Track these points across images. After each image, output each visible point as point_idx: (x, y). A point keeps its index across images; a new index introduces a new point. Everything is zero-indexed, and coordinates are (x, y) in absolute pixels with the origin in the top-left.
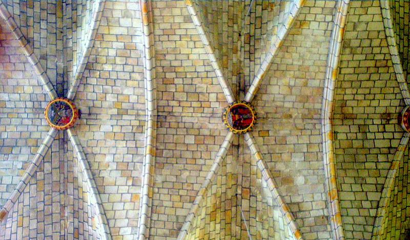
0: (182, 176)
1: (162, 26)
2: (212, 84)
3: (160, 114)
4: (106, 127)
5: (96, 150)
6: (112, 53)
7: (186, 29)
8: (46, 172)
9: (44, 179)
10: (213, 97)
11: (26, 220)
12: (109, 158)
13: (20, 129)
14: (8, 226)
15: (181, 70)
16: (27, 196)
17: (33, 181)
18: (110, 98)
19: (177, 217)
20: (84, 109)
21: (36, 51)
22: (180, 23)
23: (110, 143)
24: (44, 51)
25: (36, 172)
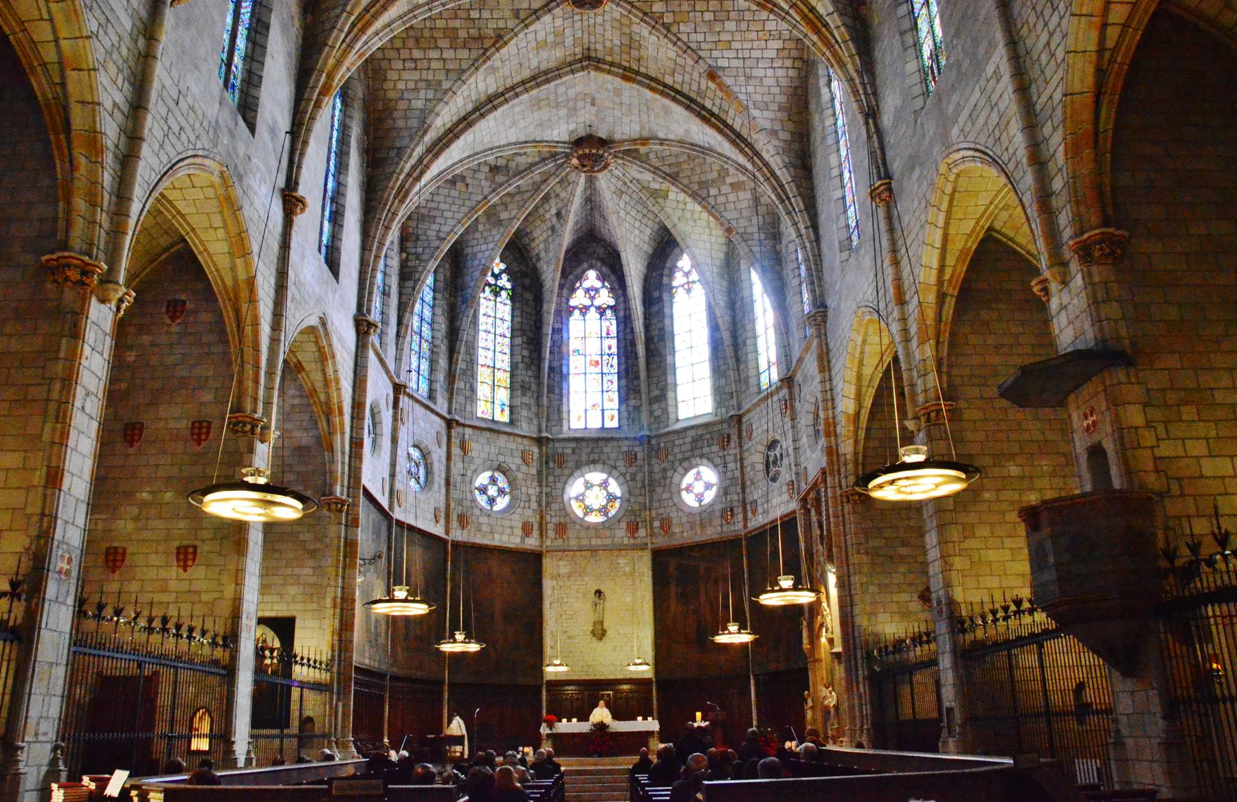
8: (664, 10)
9: (674, 12)
13: (608, 27)
16: (693, 37)
17: (674, 29)
21: (510, 24)
24: (508, 14)
25: (663, 24)
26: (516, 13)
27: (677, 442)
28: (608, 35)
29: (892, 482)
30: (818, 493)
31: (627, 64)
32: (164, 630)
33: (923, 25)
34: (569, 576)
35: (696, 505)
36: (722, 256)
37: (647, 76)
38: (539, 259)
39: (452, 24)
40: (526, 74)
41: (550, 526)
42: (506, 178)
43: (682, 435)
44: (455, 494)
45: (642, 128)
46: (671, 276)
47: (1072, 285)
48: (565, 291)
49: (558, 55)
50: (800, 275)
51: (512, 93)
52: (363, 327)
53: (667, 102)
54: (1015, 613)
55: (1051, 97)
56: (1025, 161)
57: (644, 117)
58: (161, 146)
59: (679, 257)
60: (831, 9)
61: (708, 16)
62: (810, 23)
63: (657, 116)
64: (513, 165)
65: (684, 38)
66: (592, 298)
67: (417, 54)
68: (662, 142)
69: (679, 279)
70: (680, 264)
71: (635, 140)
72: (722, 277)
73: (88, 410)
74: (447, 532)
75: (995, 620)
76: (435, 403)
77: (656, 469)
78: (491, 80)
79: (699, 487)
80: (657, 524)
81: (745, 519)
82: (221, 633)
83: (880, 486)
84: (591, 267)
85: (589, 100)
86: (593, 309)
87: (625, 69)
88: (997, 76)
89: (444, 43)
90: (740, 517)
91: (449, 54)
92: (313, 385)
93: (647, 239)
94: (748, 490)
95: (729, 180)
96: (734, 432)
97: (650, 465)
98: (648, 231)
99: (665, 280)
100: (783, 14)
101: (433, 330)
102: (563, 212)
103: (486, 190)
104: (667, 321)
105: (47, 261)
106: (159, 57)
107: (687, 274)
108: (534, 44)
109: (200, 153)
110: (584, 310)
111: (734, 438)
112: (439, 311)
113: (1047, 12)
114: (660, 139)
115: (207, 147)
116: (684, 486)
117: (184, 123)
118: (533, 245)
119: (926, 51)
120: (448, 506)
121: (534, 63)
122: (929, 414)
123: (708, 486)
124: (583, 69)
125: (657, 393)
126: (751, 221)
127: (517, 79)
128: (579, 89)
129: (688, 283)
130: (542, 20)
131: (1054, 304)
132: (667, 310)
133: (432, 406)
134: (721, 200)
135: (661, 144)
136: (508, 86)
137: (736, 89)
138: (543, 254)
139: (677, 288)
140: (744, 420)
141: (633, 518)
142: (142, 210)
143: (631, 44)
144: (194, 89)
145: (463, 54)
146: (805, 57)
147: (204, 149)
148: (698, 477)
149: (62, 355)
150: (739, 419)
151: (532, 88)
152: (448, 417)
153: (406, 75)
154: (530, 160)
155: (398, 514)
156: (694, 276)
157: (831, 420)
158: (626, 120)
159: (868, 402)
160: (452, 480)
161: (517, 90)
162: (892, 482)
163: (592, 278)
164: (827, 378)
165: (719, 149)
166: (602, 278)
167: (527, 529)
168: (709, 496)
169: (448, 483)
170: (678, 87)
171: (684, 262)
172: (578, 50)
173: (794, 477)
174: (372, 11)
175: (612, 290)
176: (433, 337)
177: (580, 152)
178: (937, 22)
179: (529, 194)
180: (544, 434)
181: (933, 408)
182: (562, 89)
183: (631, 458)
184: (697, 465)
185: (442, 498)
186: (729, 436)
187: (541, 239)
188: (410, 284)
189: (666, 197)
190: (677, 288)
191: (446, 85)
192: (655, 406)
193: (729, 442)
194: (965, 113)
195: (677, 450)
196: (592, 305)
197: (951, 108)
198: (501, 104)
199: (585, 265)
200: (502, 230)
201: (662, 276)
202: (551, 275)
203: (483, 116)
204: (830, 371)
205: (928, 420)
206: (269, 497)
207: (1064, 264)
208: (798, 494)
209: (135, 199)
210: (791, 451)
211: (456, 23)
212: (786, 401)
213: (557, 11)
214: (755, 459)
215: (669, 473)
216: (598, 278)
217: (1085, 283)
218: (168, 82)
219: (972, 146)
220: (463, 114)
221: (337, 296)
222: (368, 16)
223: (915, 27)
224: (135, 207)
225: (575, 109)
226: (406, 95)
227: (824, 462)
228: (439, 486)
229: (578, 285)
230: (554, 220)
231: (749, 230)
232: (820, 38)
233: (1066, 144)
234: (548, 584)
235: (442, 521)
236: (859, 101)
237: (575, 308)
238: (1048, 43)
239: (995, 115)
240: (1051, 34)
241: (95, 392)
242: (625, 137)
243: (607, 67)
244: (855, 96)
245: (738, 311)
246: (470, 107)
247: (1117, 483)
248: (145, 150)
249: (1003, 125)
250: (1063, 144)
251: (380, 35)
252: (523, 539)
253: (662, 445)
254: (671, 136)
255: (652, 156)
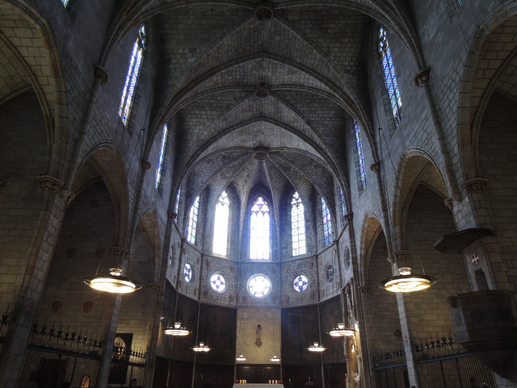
0: (298, 48)
1: (214, 63)
2: (244, 28)
3: (262, 50)
4: (270, 74)
5: (281, 80)
6: (230, 78)
7: (214, 52)
10: (251, 26)
11: (313, 109)
12: (286, 77)
13: (270, 105)
14: (314, 119)
15: (237, 47)
16: (302, 109)
17: (295, 106)
18: (254, 72)
19: (320, 60)
20: (260, 82)
21: (233, 102)
22: (212, 57)
23: (278, 74)
26: (235, 98)
27: (292, 265)
28: (269, 107)
29: (397, 284)
30: (350, 287)
31: (276, 119)
32: (73, 339)
33: (393, 102)
34: (248, 318)
35: (299, 291)
36: (310, 193)
37: (283, 123)
38: (240, 192)
39: (211, 101)
40: (238, 121)
41: (241, 298)
42: (229, 161)
43: (294, 262)
44: (203, 283)
45: (281, 143)
46: (291, 201)
47: (463, 202)
48: (250, 205)
49: (250, 115)
50: (341, 200)
51: (232, 128)
52: (171, 215)
53: (291, 133)
54: (443, 344)
55: (451, 126)
56: (440, 151)
57: (282, 140)
58: (93, 137)
59: (294, 193)
60: (356, 97)
61: (307, 101)
62: (347, 102)
63: (287, 138)
64: (232, 156)
65: (298, 109)
66: (260, 208)
67: (197, 112)
68: (288, 148)
69: (294, 201)
70: (294, 196)
71: (278, 148)
72: (311, 201)
73: (49, 242)
74: (199, 299)
75: (433, 347)
76: (197, 247)
77: (283, 276)
78: (224, 123)
79: (300, 284)
80: (283, 298)
81: (319, 297)
82: (99, 341)
83: (391, 286)
84: (260, 196)
85: (261, 132)
86: (260, 212)
87: (275, 120)
88: (426, 119)
89: (207, 108)
90: (317, 296)
91: (209, 113)
92: (149, 237)
93: (281, 186)
94: (320, 286)
95: (314, 164)
96: (314, 261)
97: (281, 274)
98: (282, 183)
99: (288, 201)
100: (337, 100)
101: (198, 218)
102: (250, 175)
103: (221, 165)
104: (289, 218)
105: (39, 179)
106: (95, 103)
107: (297, 200)
108: (241, 110)
109: (109, 141)
110: (257, 213)
111: (315, 264)
112: (201, 211)
113: (448, 93)
114: (288, 148)
115: (112, 140)
116: (294, 283)
117: (103, 129)
118: (238, 187)
119: (395, 112)
120: (200, 288)
121: (241, 117)
122: (398, 256)
123: (304, 283)
124: (259, 120)
125: (284, 245)
126: (322, 179)
127: (234, 123)
128: (257, 128)
129: (297, 203)
130: (244, 101)
131: (455, 209)
132: (289, 213)
133: (196, 248)
134: (311, 171)
135: (288, 150)
136: (231, 126)
137: (318, 129)
138: (241, 190)
139: (293, 205)
140: (319, 257)
141: (274, 295)
142: (82, 162)
143: (278, 111)
144: (108, 116)
145: (215, 113)
146: (344, 117)
147: (110, 140)
148: (300, 279)
149: (40, 218)
150: (317, 256)
151: (240, 127)
152: (202, 252)
153: (192, 120)
154: (238, 154)
155: (180, 291)
156: (300, 200)
157: (355, 258)
158: (275, 140)
159: (370, 251)
160: (202, 278)
161: (234, 127)
162: (397, 284)
163: (260, 200)
164: (353, 241)
165: (310, 152)
166: (264, 200)
167: (231, 298)
168: (305, 287)
169: (200, 279)
170: (296, 128)
171: (296, 195)
172: (258, 113)
173: (339, 281)
174: (181, 94)
175: (268, 205)
176: (198, 221)
177: (257, 152)
178: (399, 100)
179: (237, 167)
180: (239, 261)
181: (400, 253)
182: (251, 128)
183: (274, 271)
184: (300, 275)
185: (198, 284)
186: (312, 264)
187: (241, 185)
188: (189, 200)
189: (290, 170)
190: (293, 205)
191: (207, 124)
192: (284, 251)
193: (312, 266)
194: (412, 135)
195: (292, 268)
196: (260, 211)
197: (406, 133)
198: (228, 133)
199: (258, 195)
200: (226, 181)
201: (287, 200)
202: (244, 199)
203: (221, 136)
204: (354, 238)
205: (398, 258)
206: (121, 282)
207: (460, 193)
208: (341, 288)
209: (79, 157)
210: (338, 270)
211: (213, 101)
212: (336, 250)
213: (251, 98)
214: (322, 273)
215: (289, 278)
216: (263, 201)
217: (470, 201)
218: (97, 113)
219: (415, 147)
220: (213, 135)
221: (161, 202)
222: (179, 96)
223: (390, 104)
224: (79, 160)
225: (256, 135)
226: (192, 127)
227: (352, 275)
228: (197, 280)
229: (255, 203)
230: (246, 178)
231: (322, 183)
232: (351, 109)
233: (458, 144)
234: (239, 323)
235: (197, 294)
236: (366, 132)
237: (253, 212)
238: (449, 104)
239: (425, 136)
240: (450, 101)
241: (53, 234)
242: (274, 147)
243: (269, 120)
244: (365, 130)
245: (316, 214)
246: (216, 133)
247: (491, 287)
248: (86, 138)
249: (429, 138)
250: (457, 145)
251: (183, 103)
252: (229, 303)
253: (286, 266)
254: (292, 147)
255: (284, 154)
